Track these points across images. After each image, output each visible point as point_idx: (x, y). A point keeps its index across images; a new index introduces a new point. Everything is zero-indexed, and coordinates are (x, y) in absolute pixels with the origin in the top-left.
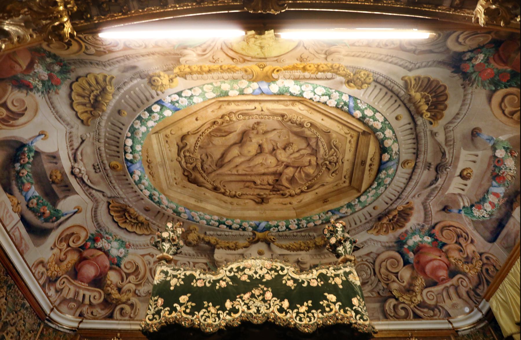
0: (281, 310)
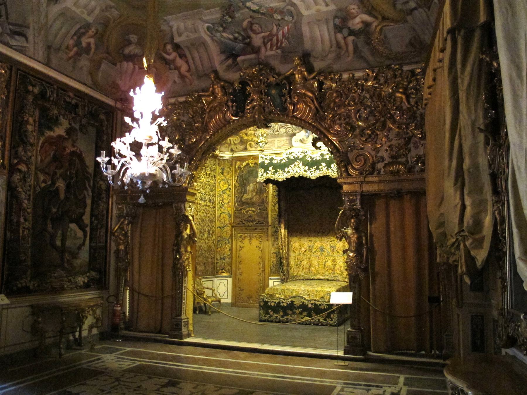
0: (305, 171)
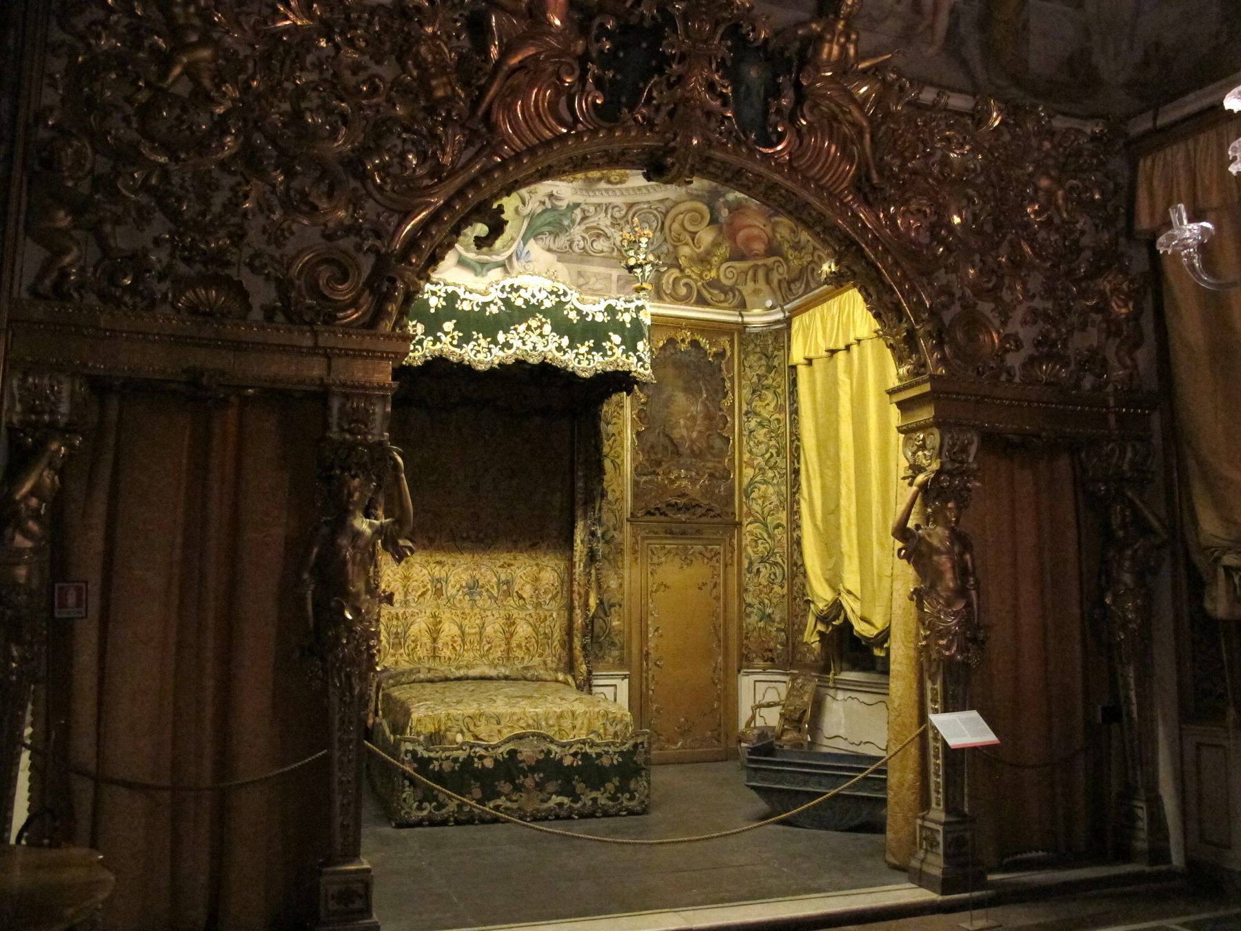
0: (559, 349)
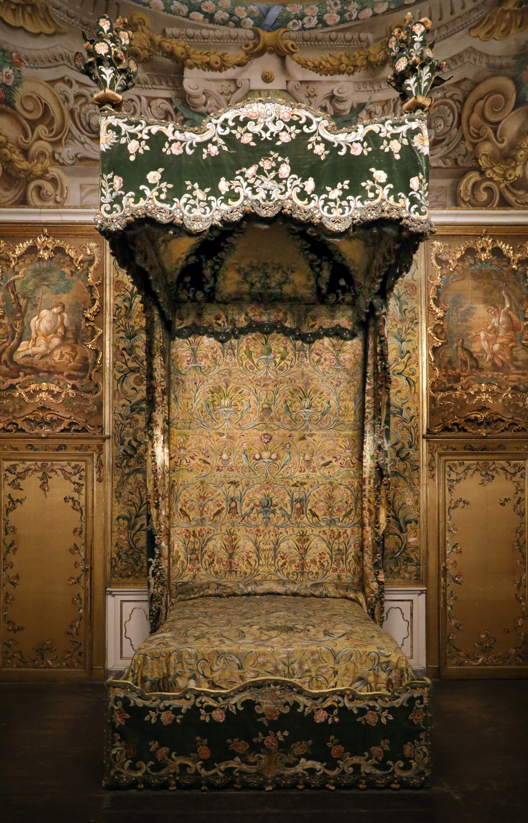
0: (302, 195)
